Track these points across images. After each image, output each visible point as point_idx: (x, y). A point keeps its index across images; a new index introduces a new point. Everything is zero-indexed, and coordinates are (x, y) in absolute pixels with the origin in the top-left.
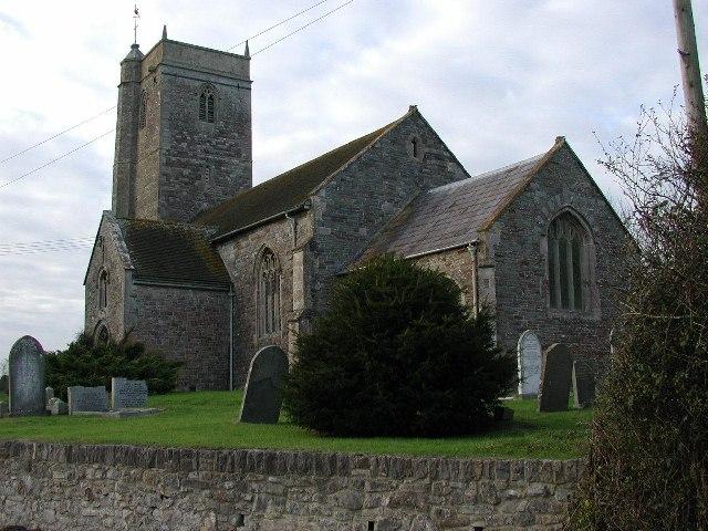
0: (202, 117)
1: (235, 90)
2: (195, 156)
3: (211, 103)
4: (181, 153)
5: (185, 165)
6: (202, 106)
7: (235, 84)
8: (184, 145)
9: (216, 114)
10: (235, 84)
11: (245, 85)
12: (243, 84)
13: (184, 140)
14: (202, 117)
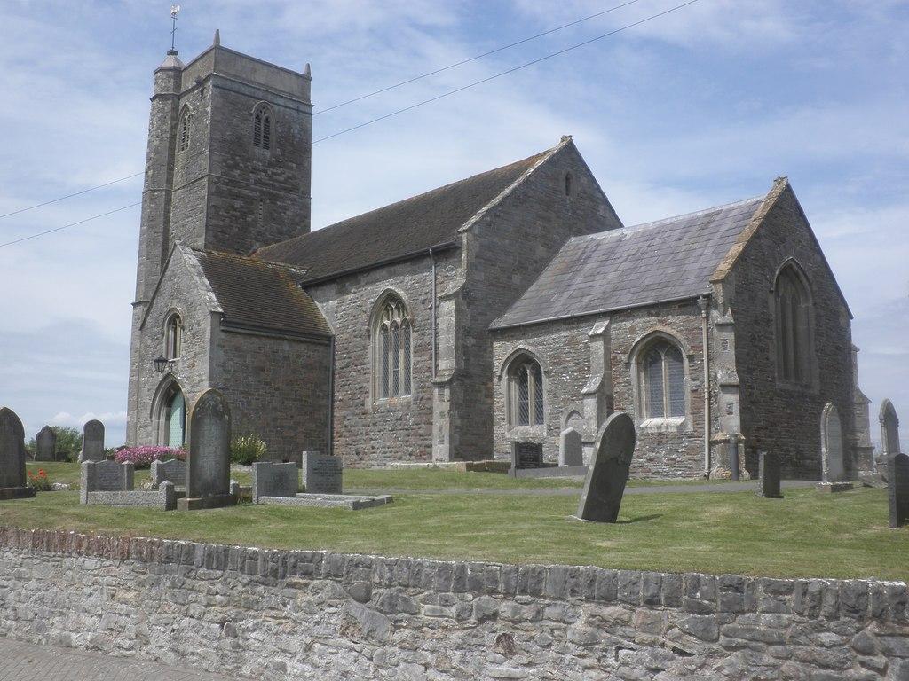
0: (257, 143)
1: (294, 113)
2: (248, 186)
3: (267, 126)
4: (233, 182)
5: (237, 197)
6: (257, 128)
7: (295, 106)
8: (237, 172)
9: (273, 138)
10: (295, 106)
11: (307, 110)
12: (302, 106)
13: (236, 166)
14: (257, 143)
